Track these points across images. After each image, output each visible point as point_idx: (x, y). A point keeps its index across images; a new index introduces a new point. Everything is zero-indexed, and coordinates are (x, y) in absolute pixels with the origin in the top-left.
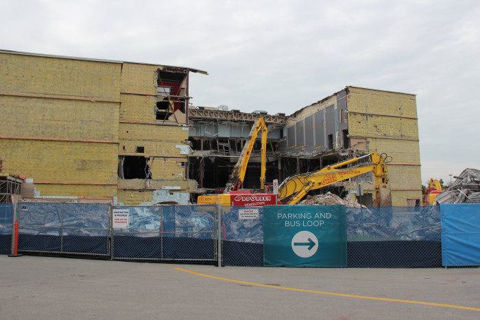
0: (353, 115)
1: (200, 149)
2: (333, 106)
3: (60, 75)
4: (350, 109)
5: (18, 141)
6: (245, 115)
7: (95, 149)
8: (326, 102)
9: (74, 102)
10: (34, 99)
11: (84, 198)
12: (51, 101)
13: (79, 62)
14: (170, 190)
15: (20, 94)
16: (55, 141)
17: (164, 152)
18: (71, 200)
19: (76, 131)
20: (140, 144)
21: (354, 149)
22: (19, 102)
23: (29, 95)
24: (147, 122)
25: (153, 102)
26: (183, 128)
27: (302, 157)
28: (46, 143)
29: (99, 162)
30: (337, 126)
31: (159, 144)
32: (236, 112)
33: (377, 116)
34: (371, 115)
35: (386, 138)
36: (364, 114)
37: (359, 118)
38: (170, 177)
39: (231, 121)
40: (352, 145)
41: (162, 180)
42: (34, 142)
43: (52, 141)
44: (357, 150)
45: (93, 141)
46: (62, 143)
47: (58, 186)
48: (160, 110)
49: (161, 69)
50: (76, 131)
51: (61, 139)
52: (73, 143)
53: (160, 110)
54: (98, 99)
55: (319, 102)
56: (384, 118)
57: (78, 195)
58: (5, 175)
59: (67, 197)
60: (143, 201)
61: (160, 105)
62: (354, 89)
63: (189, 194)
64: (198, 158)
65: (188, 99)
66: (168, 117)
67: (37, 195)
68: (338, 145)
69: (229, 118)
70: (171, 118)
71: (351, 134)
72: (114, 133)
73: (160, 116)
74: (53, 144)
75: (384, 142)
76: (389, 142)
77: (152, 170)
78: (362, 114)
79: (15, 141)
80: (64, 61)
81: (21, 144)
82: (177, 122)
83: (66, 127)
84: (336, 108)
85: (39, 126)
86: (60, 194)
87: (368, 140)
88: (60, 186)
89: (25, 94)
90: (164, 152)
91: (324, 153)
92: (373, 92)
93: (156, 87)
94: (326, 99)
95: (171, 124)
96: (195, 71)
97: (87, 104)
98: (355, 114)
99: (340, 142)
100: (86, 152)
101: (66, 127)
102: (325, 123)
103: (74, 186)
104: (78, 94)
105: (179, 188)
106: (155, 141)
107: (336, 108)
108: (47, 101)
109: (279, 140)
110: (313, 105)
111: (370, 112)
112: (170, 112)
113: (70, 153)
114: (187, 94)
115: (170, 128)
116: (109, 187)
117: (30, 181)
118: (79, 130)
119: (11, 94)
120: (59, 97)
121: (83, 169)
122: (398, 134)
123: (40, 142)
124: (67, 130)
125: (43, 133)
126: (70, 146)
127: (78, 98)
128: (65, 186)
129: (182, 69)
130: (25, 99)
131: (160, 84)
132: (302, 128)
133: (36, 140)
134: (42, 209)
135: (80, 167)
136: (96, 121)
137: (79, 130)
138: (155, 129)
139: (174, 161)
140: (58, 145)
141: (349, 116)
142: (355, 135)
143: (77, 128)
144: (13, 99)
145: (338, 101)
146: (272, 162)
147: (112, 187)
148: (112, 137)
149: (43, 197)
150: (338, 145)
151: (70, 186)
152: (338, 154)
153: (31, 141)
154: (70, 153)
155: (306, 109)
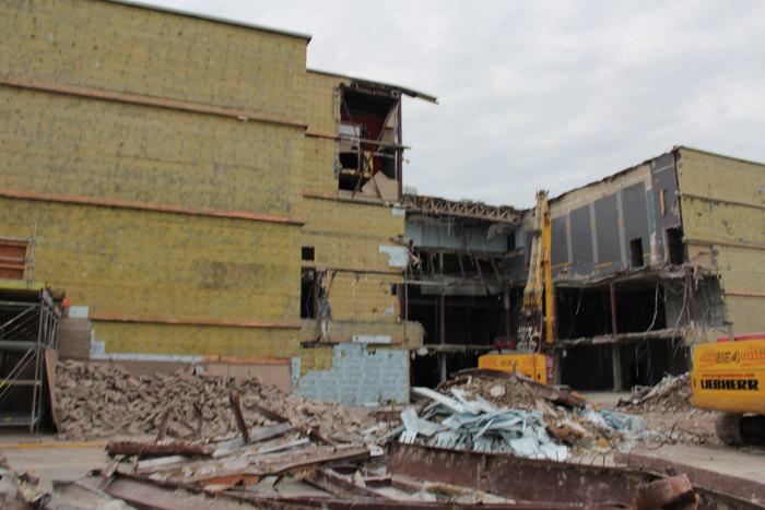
2: (641, 185)
3: (164, 52)
4: (686, 187)
5: (53, 206)
6: (453, 204)
7: (246, 235)
8: (623, 178)
9: (195, 118)
10: (97, 104)
11: (219, 362)
12: (140, 110)
13: (211, 26)
14: (370, 345)
15: (65, 89)
16: (147, 210)
17: (355, 261)
18: (187, 366)
19: (201, 188)
20: (309, 242)
21: (694, 264)
22: (59, 107)
23: (84, 91)
24: (319, 192)
25: (332, 151)
26: (394, 211)
27: (562, 285)
28: (125, 214)
29: (256, 268)
30: (652, 223)
31: (344, 242)
32: (440, 202)
33: (727, 204)
34: (717, 203)
35: (742, 246)
37: (698, 205)
38: (368, 316)
39: (429, 215)
40: (690, 257)
41: (351, 322)
42: (93, 210)
43: (139, 209)
44: (699, 267)
45: (242, 215)
46: (164, 216)
47: (153, 329)
48: (344, 171)
49: (348, 84)
50: (201, 188)
51: (164, 207)
52: (193, 219)
53: (344, 171)
54: (254, 116)
55: (605, 180)
56: (737, 208)
57: (204, 353)
58: (36, 286)
59: (176, 358)
60: (311, 368)
61: (347, 160)
62: (691, 154)
63: (407, 352)
65: (401, 150)
66: (362, 185)
67: (99, 351)
68: (655, 257)
69: (425, 209)
70: (367, 189)
71: (687, 236)
72: (292, 199)
73: (347, 183)
74: (142, 219)
75: (739, 254)
77: (332, 301)
79: (44, 206)
80: (177, 20)
81: (61, 212)
82: (379, 196)
83: (176, 177)
84: (649, 187)
85: (108, 173)
86: (157, 349)
87: (716, 248)
88: (159, 328)
89: (76, 90)
90: (355, 261)
91: (619, 274)
92: (717, 159)
93: (337, 121)
94: (624, 173)
95: (369, 200)
96: (413, 94)
97: (229, 125)
98: (692, 198)
99: (660, 251)
100: (224, 242)
101: (176, 177)
102: (621, 218)
103: (194, 330)
104: (206, 100)
105: (386, 339)
106: (337, 235)
107: (649, 187)
108: (132, 109)
109: (504, 254)
110: (589, 185)
111: (715, 195)
112: (367, 175)
113: (184, 244)
114: (400, 140)
115: (368, 208)
116: (282, 334)
117: (78, 312)
118: (209, 188)
119: (38, 85)
120: (161, 102)
121: (216, 286)
123: (109, 212)
124: (178, 185)
125: (118, 188)
126: (186, 227)
127: (208, 109)
128: (170, 329)
129: (389, 88)
130: (75, 101)
131: (345, 119)
132: (563, 230)
133: (99, 206)
134: (114, 388)
135: (210, 280)
136: (248, 168)
137: (209, 188)
138: (336, 208)
139: (376, 280)
140: (156, 222)
141: (682, 201)
142: (699, 237)
143: (203, 181)
144: (42, 99)
145: (654, 176)
146: (496, 296)
147: (289, 332)
148: (289, 209)
149: (114, 356)
150: (655, 257)
151: (183, 329)
152: (659, 278)
153: (84, 209)
154: (184, 244)
155: (570, 197)
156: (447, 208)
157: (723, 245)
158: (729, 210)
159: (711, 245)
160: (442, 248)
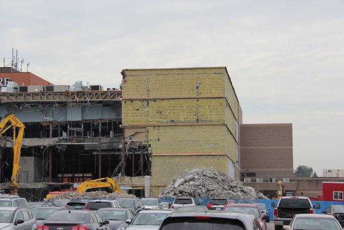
0: (129, 103)
1: (48, 136)
34: (155, 100)
35: (173, 124)
36: (144, 100)
39: (73, 102)
56: (172, 101)
62: (132, 73)
64: (42, 148)
75: (170, 131)
76: (178, 130)
78: (140, 100)
98: (132, 101)
111: (153, 95)
122: (192, 118)
156: (85, 98)
157: (154, 127)
158: (165, 103)
159: (144, 127)
160: (100, 120)
